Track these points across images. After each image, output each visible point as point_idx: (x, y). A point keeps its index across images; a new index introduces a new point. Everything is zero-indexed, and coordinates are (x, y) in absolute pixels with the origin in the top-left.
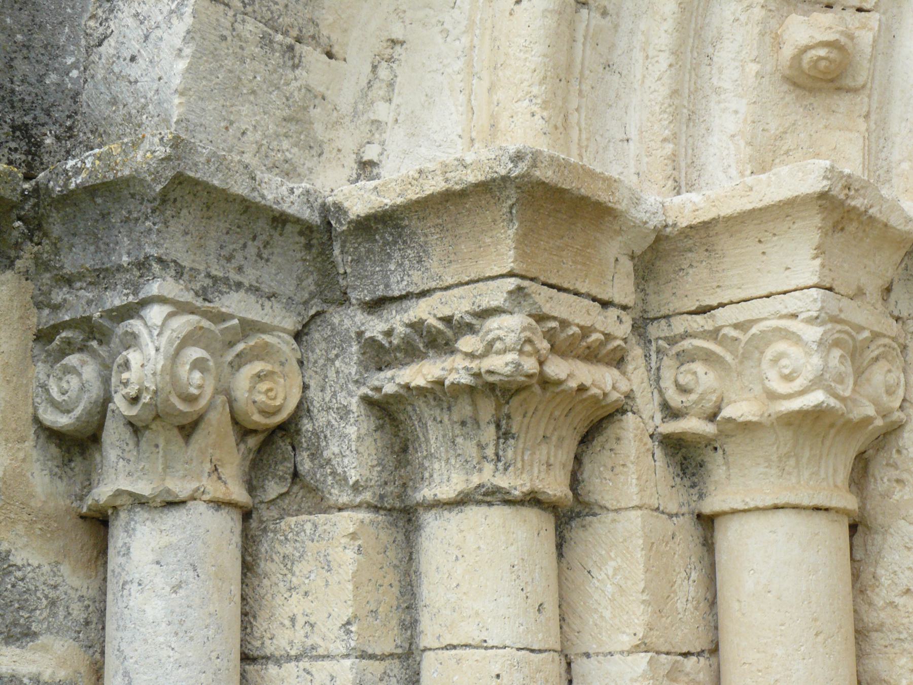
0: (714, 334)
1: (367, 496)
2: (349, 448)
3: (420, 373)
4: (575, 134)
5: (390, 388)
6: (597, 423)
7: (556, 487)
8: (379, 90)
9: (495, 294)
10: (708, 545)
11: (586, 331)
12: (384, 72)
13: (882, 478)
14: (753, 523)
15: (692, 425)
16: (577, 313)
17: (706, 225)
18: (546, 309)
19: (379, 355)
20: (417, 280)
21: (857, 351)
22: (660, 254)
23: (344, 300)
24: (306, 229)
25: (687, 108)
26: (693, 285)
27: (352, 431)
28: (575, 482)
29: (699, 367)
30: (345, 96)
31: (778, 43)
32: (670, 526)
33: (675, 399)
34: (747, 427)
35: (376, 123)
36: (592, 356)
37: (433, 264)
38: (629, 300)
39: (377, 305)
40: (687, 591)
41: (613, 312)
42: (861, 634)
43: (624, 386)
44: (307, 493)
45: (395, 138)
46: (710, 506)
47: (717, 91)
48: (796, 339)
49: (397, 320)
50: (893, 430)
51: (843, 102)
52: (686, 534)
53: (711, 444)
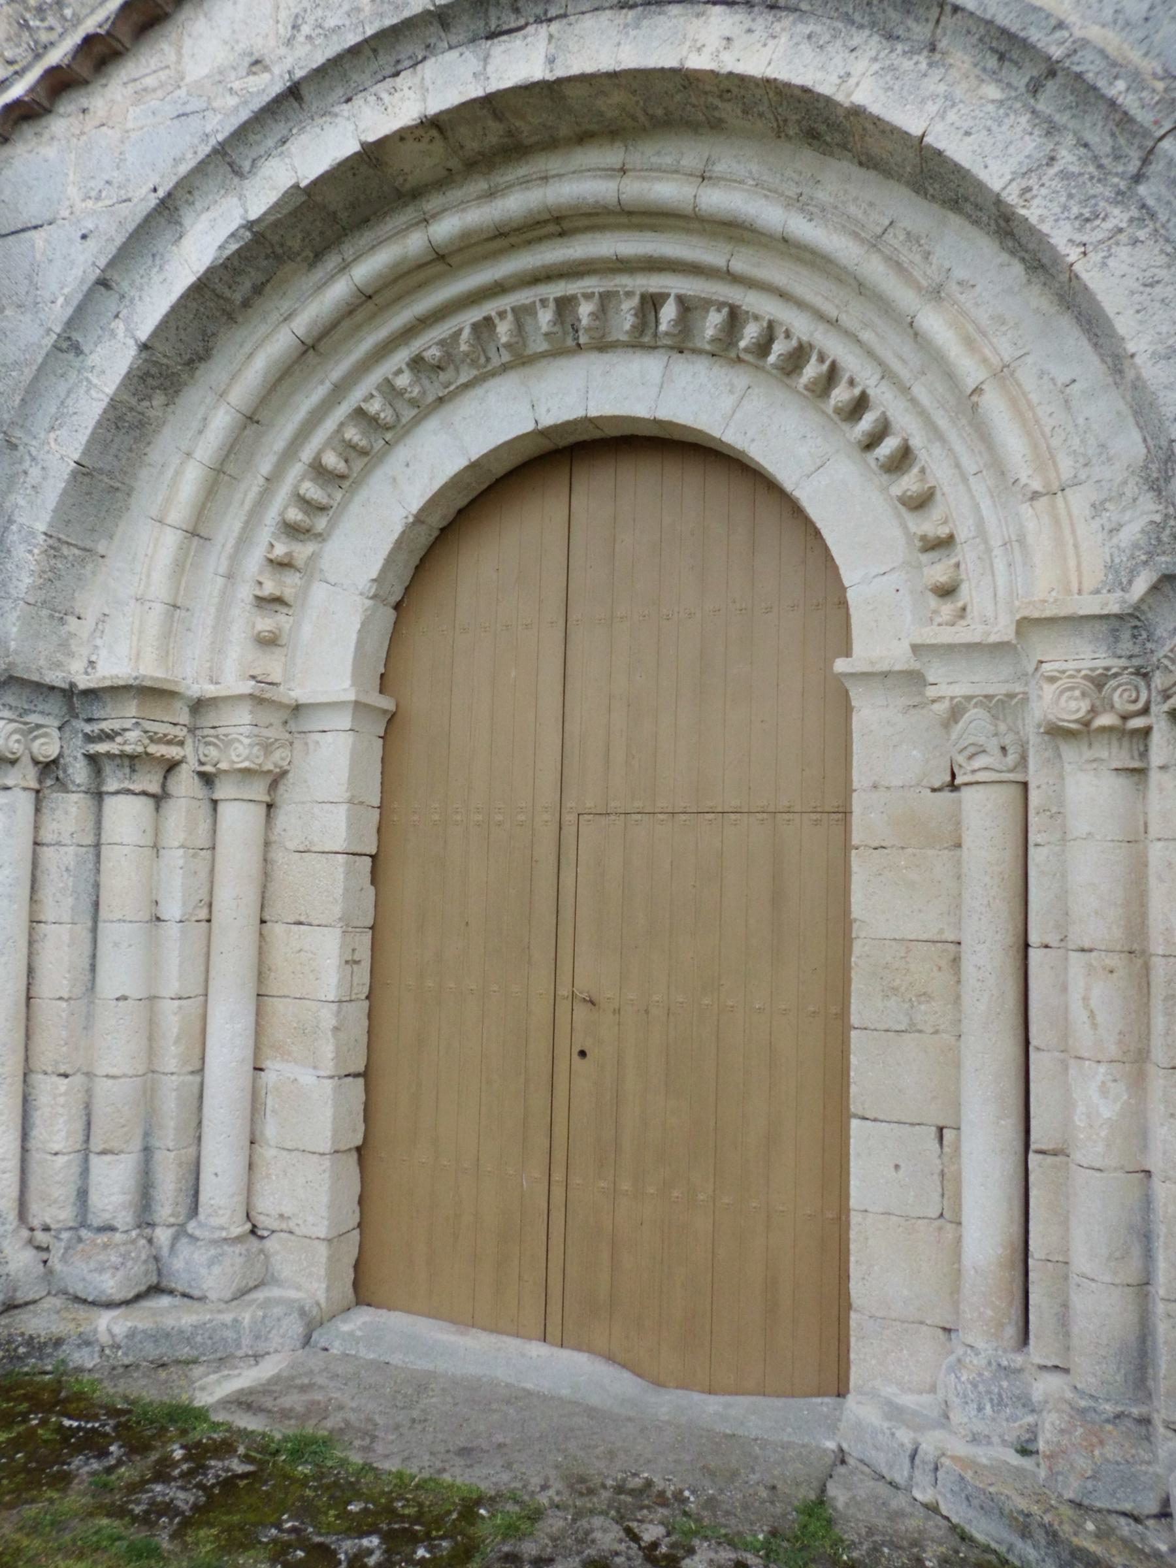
0: (217, 737)
1: (83, 788)
2: (79, 772)
4: (171, 658)
5: (92, 752)
6: (172, 766)
7: (154, 788)
8: (98, 634)
9: (128, 724)
10: (215, 810)
11: (165, 735)
12: (100, 627)
13: (281, 788)
14: (227, 803)
15: (208, 768)
16: (162, 729)
17: (215, 698)
18: (148, 729)
19: (89, 738)
21: (267, 747)
22: (199, 706)
23: (77, 717)
24: (62, 690)
25: (217, 649)
26: (210, 718)
27: (78, 765)
28: (164, 786)
29: (211, 748)
30: (85, 635)
31: (254, 627)
32: (198, 803)
33: (203, 759)
34: (225, 771)
35: (96, 647)
36: (169, 743)
37: (108, 709)
38: (187, 723)
39: (89, 720)
40: (204, 826)
41: (178, 727)
42: (267, 844)
43: (182, 754)
44: (62, 785)
45: (103, 653)
46: (215, 797)
47: (231, 642)
48: (241, 742)
50: (284, 773)
51: (278, 650)
52: (206, 807)
53: (215, 775)
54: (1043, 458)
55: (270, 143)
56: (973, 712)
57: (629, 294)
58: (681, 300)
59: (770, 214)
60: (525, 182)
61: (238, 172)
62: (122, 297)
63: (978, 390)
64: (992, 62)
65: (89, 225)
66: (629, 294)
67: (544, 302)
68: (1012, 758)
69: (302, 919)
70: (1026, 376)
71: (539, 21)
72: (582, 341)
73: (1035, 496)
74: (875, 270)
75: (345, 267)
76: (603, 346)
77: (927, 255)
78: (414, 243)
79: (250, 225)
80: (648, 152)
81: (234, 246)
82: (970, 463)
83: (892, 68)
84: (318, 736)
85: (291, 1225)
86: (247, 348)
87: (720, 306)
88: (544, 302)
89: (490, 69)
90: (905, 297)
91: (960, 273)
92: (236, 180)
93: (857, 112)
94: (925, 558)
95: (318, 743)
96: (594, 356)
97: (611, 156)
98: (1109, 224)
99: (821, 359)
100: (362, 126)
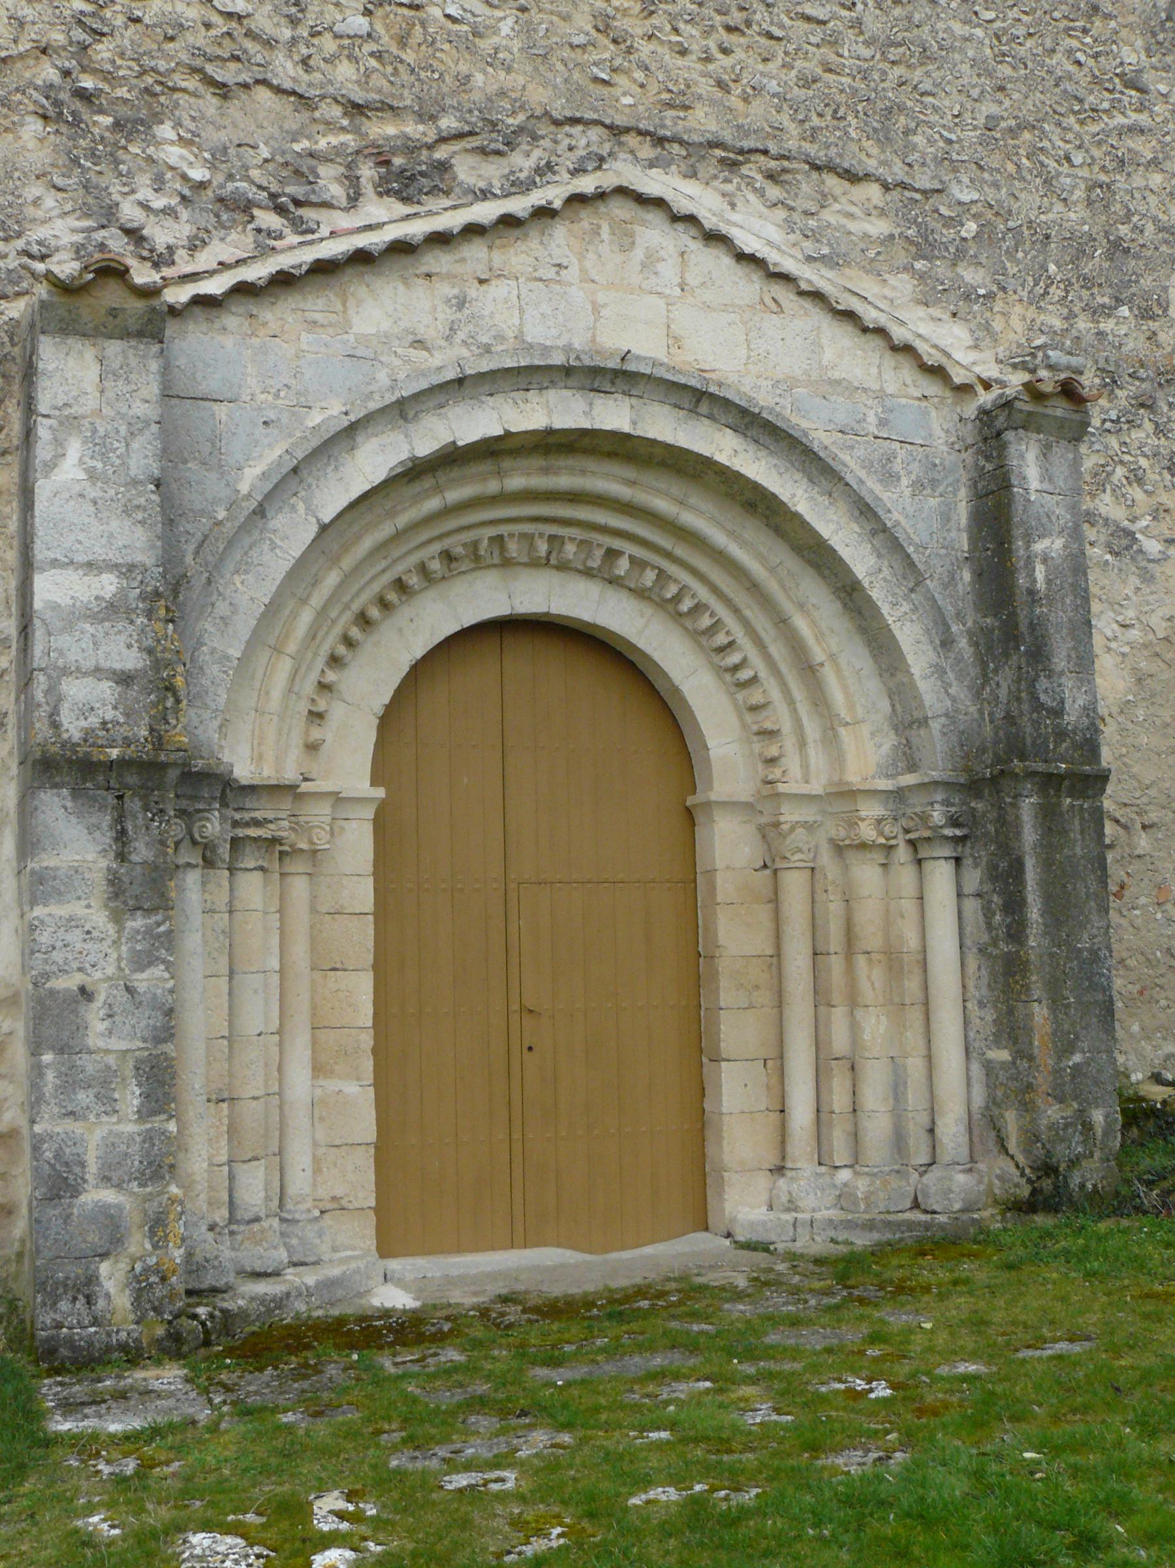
3: (253, 832)
19: (236, 824)
20: (256, 805)
23: (227, 806)
34: (302, 850)
39: (236, 810)
45: (226, 751)
49: (247, 816)
54: (851, 707)
55: (431, 404)
56: (800, 830)
57: (599, 545)
58: (630, 556)
59: (720, 538)
60: (571, 471)
61: (403, 416)
62: (301, 482)
63: (822, 665)
64: (857, 513)
65: (272, 415)
66: (599, 545)
67: (541, 535)
68: (811, 855)
69: (338, 966)
70: (843, 661)
71: (624, 393)
72: (553, 561)
73: (847, 724)
74: (772, 586)
75: (438, 489)
76: (563, 567)
77: (798, 585)
78: (493, 486)
79: (414, 459)
80: (649, 477)
81: (399, 470)
82: (798, 694)
83: (813, 498)
84: (342, 823)
85: (344, 1203)
86: (356, 528)
87: (654, 567)
88: (541, 535)
89: (595, 412)
90: (787, 606)
91: (813, 600)
92: (401, 422)
93: (797, 515)
94: (755, 738)
95: (342, 828)
96: (554, 572)
97: (630, 473)
98: (903, 609)
99: (712, 615)
100: (505, 418)
